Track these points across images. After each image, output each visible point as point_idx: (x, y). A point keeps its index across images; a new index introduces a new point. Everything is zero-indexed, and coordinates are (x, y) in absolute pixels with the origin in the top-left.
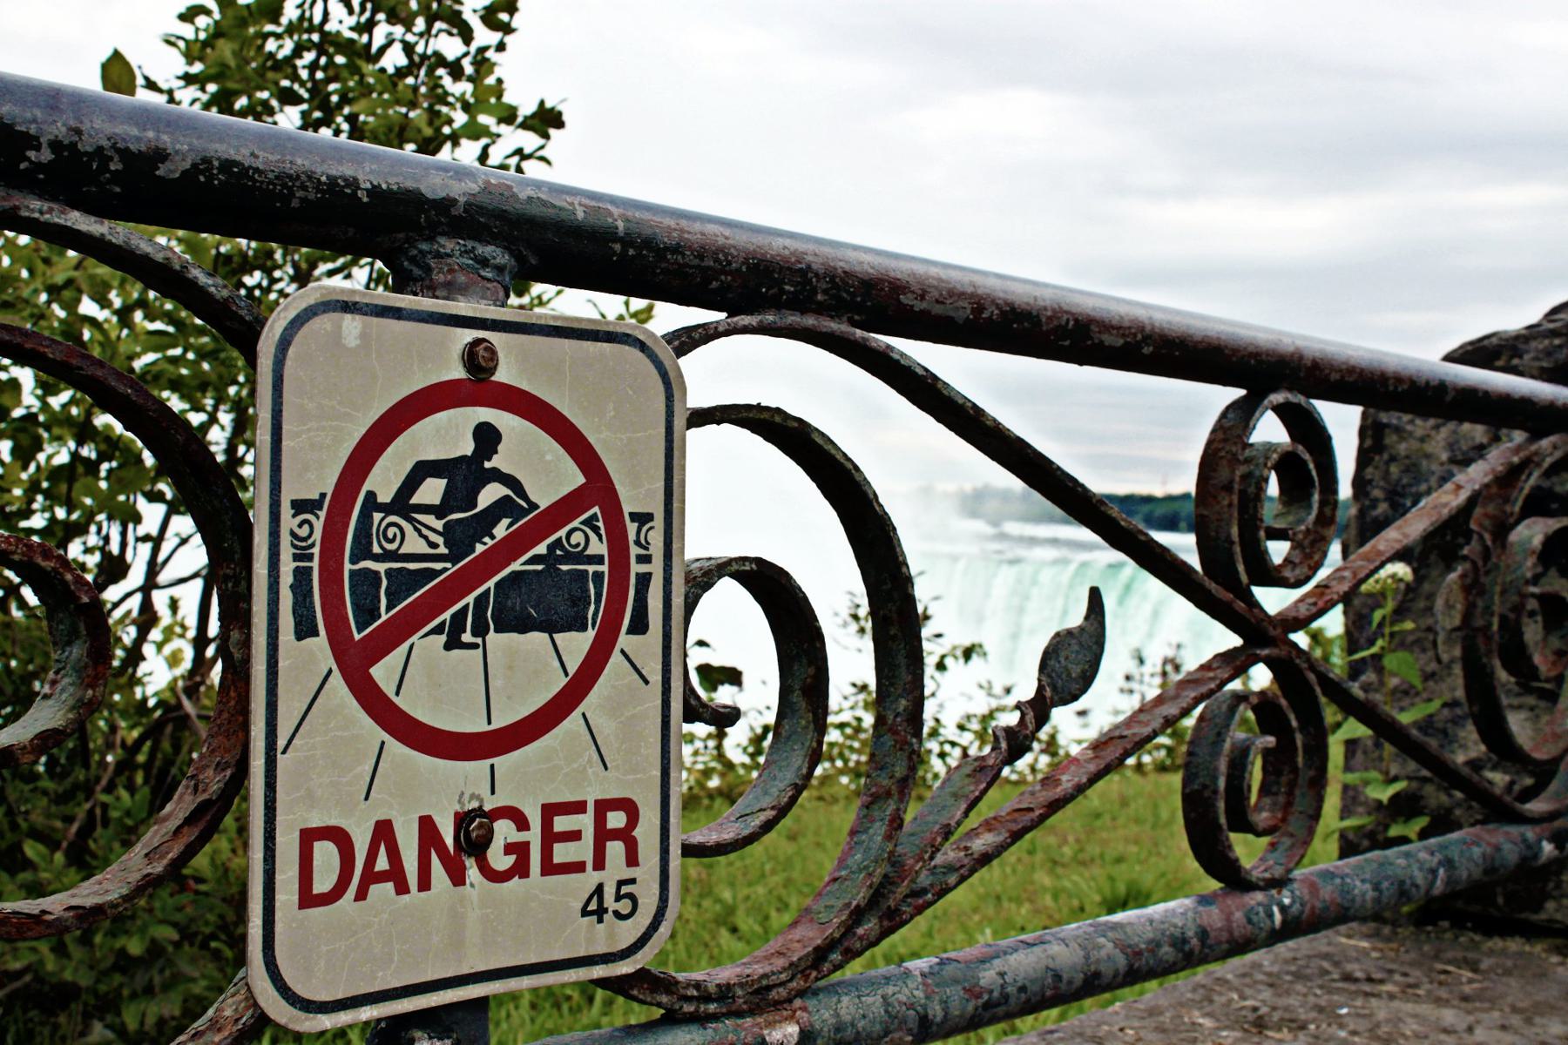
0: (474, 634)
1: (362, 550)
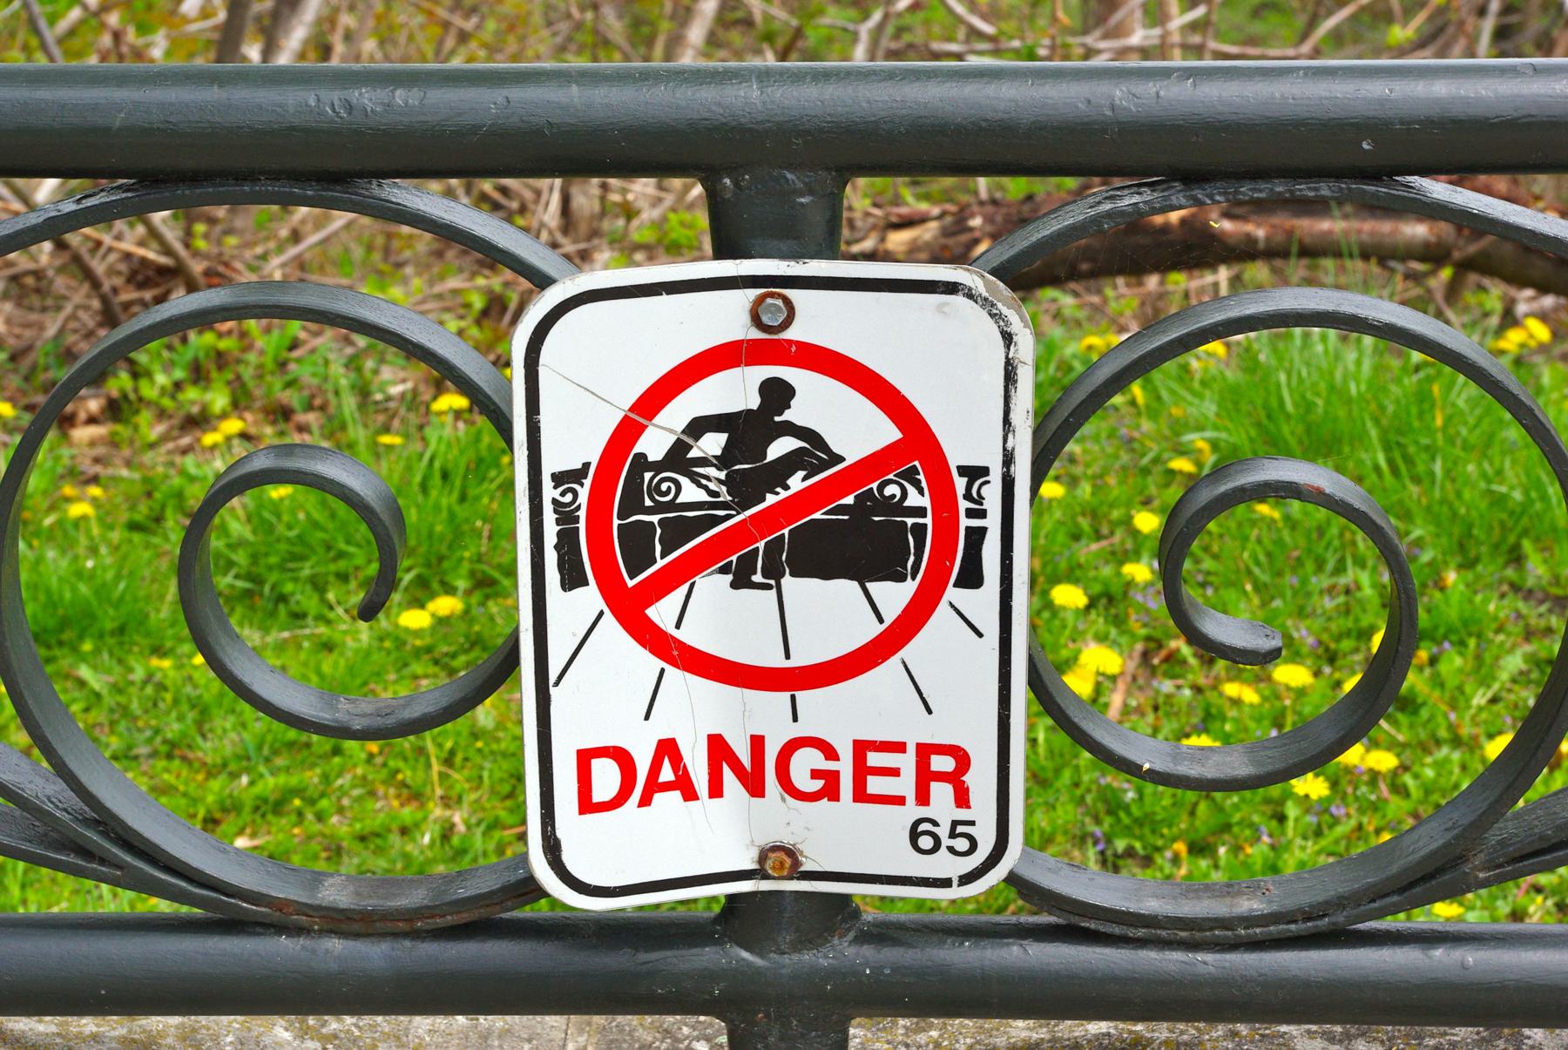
1: (632, 503)
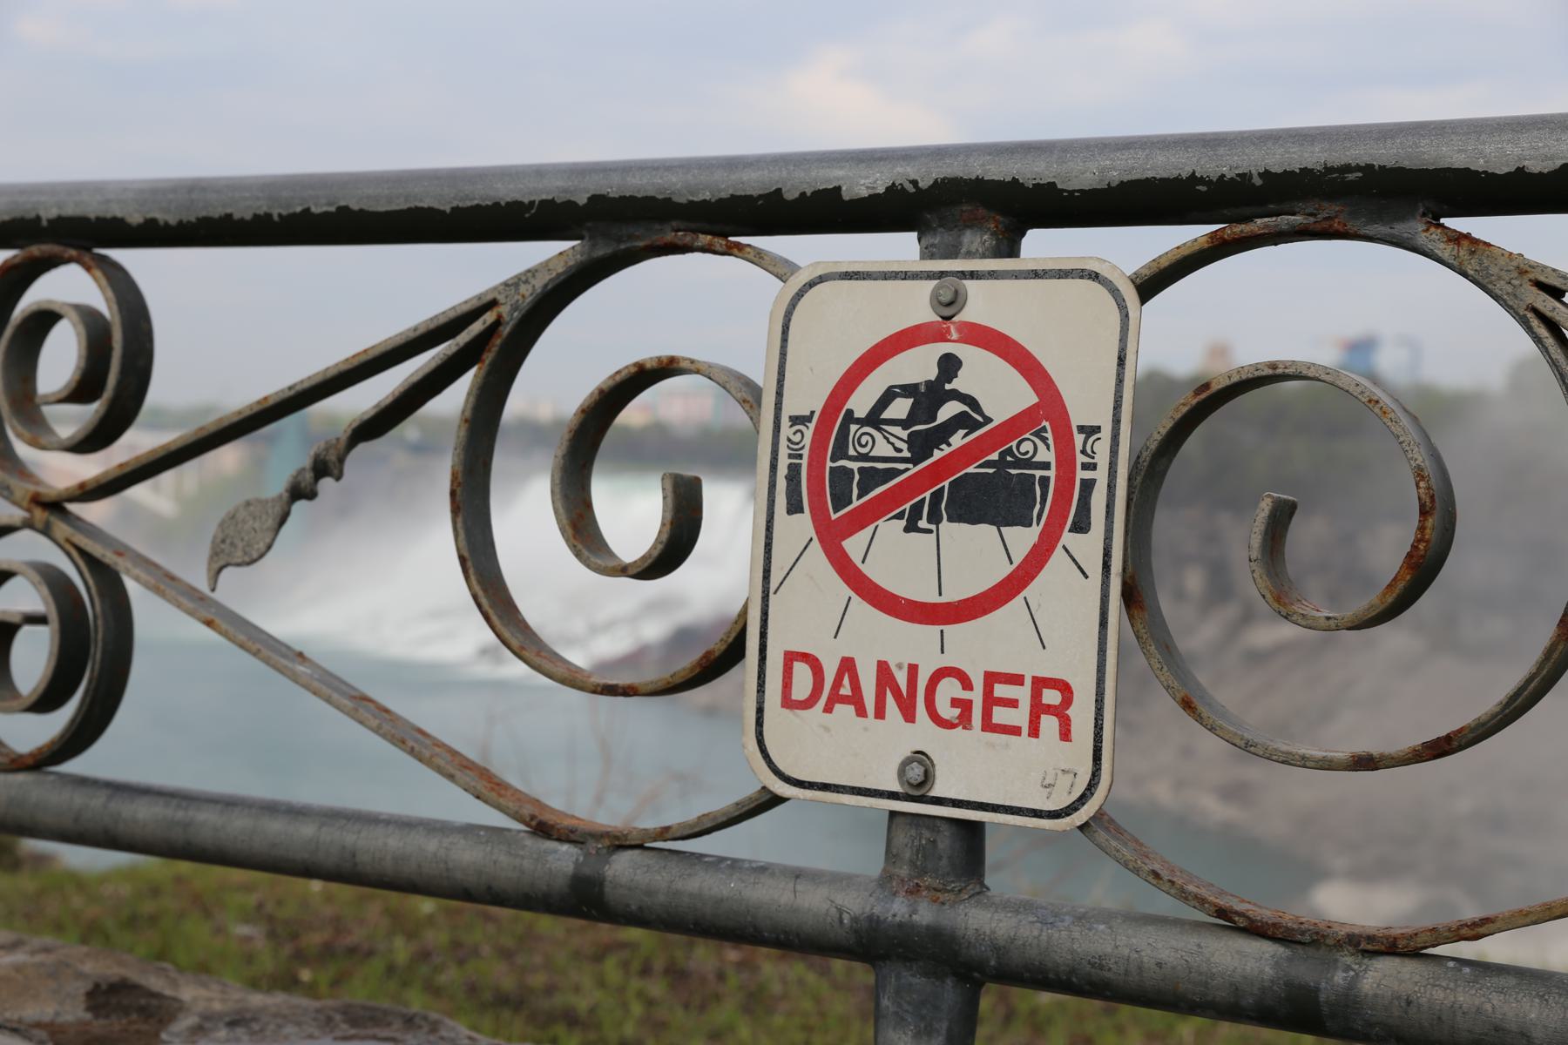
0: (929, 521)
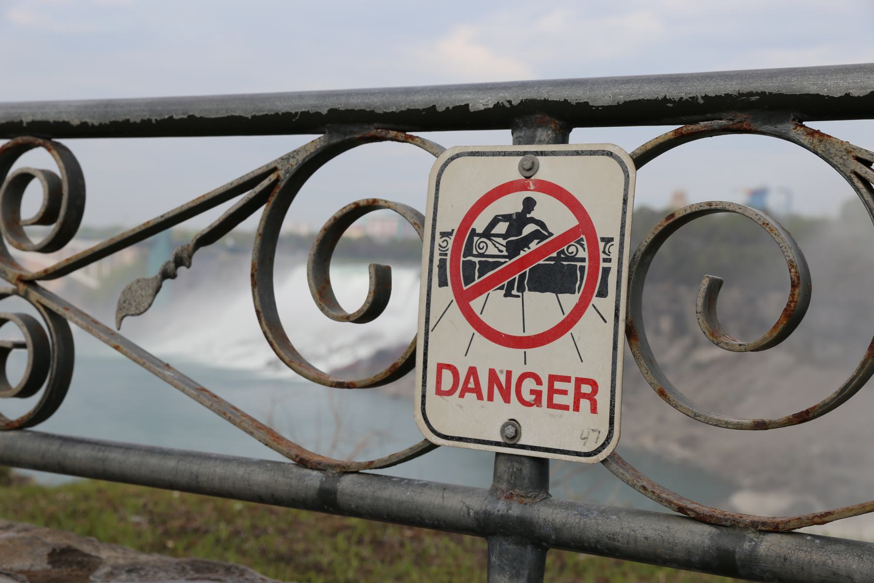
0: (518, 291)
1: (469, 252)
